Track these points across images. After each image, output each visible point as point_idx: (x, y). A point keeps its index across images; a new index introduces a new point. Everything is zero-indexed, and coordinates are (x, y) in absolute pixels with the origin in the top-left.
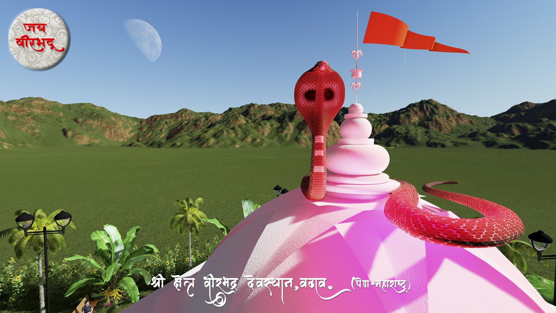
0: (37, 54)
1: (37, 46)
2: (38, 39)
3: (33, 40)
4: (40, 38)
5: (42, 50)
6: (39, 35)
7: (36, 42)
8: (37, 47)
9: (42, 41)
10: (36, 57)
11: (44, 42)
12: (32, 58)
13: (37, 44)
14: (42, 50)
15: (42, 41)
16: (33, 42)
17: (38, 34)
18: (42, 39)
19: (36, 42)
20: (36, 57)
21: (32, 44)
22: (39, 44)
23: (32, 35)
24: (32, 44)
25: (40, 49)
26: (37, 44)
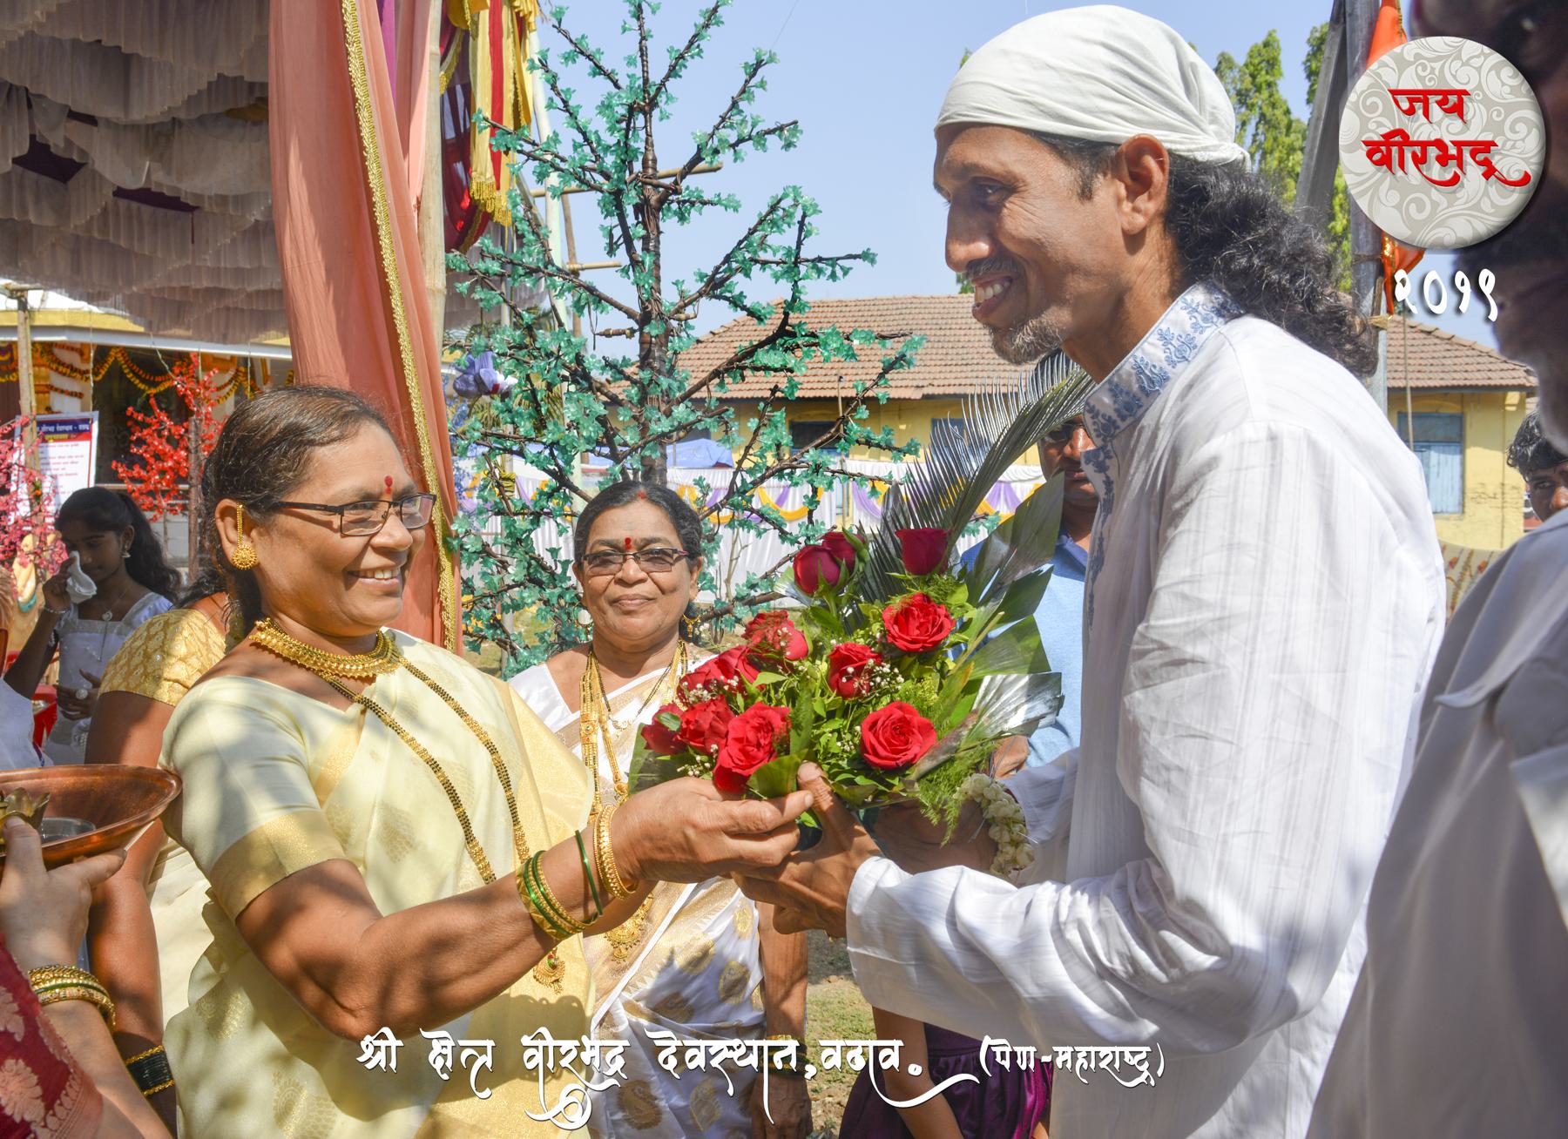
0: (1436, 193)
1: (1437, 165)
2: (1439, 144)
3: (1424, 145)
4: (1447, 140)
5: (1455, 180)
6: (1444, 127)
7: (1433, 152)
8: (1436, 171)
9: (1453, 151)
10: (1435, 204)
11: (1460, 152)
12: (1420, 209)
13: (1438, 158)
14: (1455, 180)
15: (1453, 151)
16: (1424, 152)
17: (1439, 124)
18: (1459, 144)
19: (1433, 152)
20: (1435, 204)
21: (1419, 161)
22: (1443, 160)
23: (1420, 129)
24: (1419, 161)
25: (1448, 176)
26: (1438, 158)
